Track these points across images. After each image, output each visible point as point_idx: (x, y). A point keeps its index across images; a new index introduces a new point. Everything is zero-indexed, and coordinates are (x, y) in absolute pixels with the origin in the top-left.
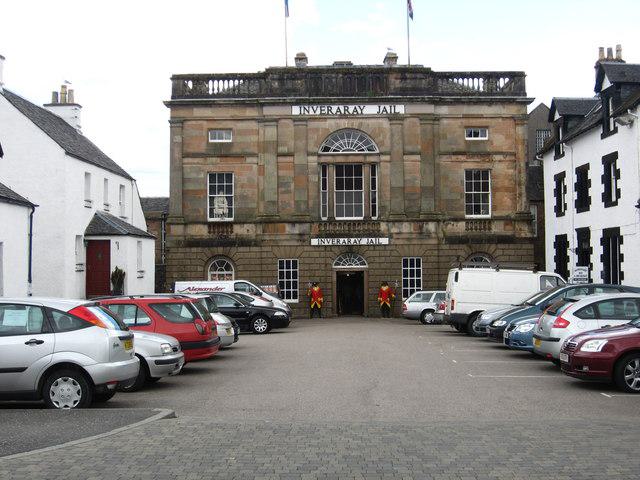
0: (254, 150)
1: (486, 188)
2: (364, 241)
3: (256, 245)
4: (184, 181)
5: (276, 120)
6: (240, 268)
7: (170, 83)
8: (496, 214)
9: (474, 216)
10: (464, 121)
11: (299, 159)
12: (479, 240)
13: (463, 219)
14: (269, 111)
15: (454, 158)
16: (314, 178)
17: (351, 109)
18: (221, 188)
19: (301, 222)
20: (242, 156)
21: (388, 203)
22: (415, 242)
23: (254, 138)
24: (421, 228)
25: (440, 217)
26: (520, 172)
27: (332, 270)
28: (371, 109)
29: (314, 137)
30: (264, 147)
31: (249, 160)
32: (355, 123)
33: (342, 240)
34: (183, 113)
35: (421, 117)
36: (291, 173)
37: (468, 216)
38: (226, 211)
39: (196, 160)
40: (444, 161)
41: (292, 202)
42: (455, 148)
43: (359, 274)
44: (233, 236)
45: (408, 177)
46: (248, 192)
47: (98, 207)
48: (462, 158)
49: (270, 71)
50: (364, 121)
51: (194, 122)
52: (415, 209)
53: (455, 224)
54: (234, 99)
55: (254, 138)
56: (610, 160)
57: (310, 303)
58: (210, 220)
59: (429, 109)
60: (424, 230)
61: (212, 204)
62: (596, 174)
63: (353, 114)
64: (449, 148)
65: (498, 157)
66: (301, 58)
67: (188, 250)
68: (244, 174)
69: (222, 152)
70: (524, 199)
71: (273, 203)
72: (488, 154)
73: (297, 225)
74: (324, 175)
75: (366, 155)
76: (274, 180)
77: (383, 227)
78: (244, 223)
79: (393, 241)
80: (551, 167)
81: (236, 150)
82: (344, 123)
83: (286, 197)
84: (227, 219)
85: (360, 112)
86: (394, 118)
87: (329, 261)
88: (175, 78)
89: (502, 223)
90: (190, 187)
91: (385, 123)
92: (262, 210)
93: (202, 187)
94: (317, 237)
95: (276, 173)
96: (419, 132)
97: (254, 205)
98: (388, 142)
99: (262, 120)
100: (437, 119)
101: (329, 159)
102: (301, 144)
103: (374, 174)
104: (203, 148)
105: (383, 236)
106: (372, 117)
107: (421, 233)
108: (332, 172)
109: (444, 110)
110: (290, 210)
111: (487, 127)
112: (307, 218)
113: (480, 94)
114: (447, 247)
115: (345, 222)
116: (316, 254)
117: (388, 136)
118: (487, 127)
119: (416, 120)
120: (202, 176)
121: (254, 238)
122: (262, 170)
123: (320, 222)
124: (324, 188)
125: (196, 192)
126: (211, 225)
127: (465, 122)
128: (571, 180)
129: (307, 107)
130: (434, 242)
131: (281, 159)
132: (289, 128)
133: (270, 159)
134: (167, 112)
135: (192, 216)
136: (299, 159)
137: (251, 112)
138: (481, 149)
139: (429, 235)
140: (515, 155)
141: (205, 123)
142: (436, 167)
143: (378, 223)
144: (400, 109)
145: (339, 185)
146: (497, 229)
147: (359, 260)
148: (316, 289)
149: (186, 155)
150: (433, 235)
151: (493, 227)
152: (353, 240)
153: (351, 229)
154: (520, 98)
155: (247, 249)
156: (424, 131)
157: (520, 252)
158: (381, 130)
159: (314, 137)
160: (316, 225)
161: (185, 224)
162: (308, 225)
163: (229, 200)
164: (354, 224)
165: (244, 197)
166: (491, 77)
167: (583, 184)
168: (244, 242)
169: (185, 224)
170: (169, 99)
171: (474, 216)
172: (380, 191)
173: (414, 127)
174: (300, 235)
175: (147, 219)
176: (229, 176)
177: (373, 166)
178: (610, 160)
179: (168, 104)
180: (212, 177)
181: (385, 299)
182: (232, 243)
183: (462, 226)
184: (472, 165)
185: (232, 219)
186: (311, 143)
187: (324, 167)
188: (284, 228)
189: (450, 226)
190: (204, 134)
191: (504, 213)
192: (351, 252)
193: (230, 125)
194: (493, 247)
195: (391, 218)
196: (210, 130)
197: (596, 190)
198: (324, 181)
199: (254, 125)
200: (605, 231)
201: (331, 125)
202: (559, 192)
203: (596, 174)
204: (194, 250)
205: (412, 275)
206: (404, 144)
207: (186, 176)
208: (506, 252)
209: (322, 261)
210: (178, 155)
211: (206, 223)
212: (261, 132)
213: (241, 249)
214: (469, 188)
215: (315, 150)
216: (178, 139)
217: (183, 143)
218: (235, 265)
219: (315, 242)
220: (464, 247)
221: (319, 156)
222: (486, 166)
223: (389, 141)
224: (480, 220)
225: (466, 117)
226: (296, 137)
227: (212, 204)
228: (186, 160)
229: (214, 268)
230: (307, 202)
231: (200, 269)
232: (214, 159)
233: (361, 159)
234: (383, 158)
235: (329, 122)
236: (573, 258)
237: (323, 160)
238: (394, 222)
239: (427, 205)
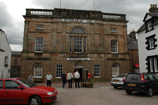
0: (50, 31)
2: (83, 59)
4: (28, 40)
6: (44, 67)
7: (25, 11)
8: (120, 52)
9: (113, 53)
10: (110, 26)
11: (64, 34)
13: (111, 53)
14: (55, 20)
15: (108, 36)
17: (79, 20)
19: (63, 53)
20: (46, 33)
21: (90, 48)
24: (100, 55)
25: (105, 53)
26: (125, 41)
28: (85, 21)
30: (53, 30)
31: (48, 34)
32: (80, 25)
33: (76, 59)
35: (99, 24)
36: (61, 38)
37: (112, 53)
39: (32, 34)
40: (106, 37)
41: (61, 47)
44: (42, 57)
48: (110, 36)
49: (55, 9)
50: (83, 24)
51: (32, 23)
52: (98, 50)
53: (109, 54)
55: (50, 28)
58: (35, 52)
59: (101, 22)
60: (100, 56)
63: (80, 22)
64: (106, 33)
67: (28, 61)
69: (41, 32)
70: (127, 48)
71: (56, 47)
72: (117, 35)
75: (83, 34)
77: (88, 55)
78: (46, 53)
81: (44, 31)
82: (77, 25)
84: (40, 52)
85: (82, 21)
86: (91, 24)
87: (72, 65)
88: (27, 10)
89: (121, 55)
90: (29, 41)
91: (89, 25)
92: (51, 49)
93: (34, 42)
94: (69, 57)
95: (56, 38)
96: (98, 28)
100: (103, 25)
101: (72, 35)
103: (85, 40)
104: (34, 31)
107: (100, 57)
109: (105, 23)
110: (60, 50)
111: (116, 28)
114: (107, 61)
116: (68, 63)
117: (90, 29)
118: (116, 28)
120: (34, 38)
121: (49, 58)
122: (52, 37)
126: (36, 53)
127: (111, 26)
129: (66, 19)
130: (104, 60)
131: (58, 34)
132: (60, 25)
133: (55, 34)
134: (24, 20)
135: (30, 50)
136: (64, 34)
138: (115, 34)
139: (102, 58)
140: (124, 36)
141: (35, 23)
143: (87, 54)
144: (93, 21)
146: (120, 56)
147: (81, 65)
149: (28, 32)
151: (119, 56)
152: (80, 59)
155: (47, 61)
156: (100, 28)
157: (126, 63)
160: (68, 54)
161: (28, 53)
162: (66, 54)
164: (80, 54)
165: (46, 45)
168: (46, 59)
169: (28, 53)
170: (25, 15)
171: (113, 53)
172: (87, 44)
174: (63, 57)
176: (42, 39)
179: (24, 16)
181: (89, 77)
182: (41, 59)
183: (111, 55)
184: (113, 38)
185: (42, 52)
189: (107, 56)
190: (35, 25)
191: (122, 52)
193: (43, 24)
195: (91, 52)
196: (37, 25)
199: (50, 24)
201: (73, 25)
204: (30, 61)
205: (97, 70)
206: (94, 31)
207: (29, 38)
208: (123, 63)
210: (26, 32)
211: (34, 53)
212: (52, 26)
213: (45, 61)
215: (68, 32)
216: (27, 27)
217: (28, 29)
218: (42, 66)
219: (68, 59)
222: (117, 39)
223: (90, 30)
225: (111, 25)
228: (29, 33)
229: (36, 67)
230: (65, 47)
234: (89, 35)
235: (72, 24)
237: (71, 35)
238: (92, 53)
239: (101, 49)
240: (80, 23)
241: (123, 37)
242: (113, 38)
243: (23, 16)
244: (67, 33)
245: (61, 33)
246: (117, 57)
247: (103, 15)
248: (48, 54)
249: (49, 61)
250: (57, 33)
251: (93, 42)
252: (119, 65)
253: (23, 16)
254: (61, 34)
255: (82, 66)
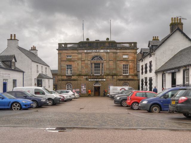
0: (77, 60)
1: (127, 68)
2: (100, 80)
3: (77, 81)
5: (81, 53)
10: (123, 53)
11: (86, 62)
12: (125, 80)
13: (122, 75)
14: (80, 51)
15: (120, 62)
16: (89, 66)
17: (98, 51)
18: (69, 68)
20: (73, 61)
22: (111, 80)
23: (76, 57)
24: (113, 77)
27: (93, 86)
28: (102, 51)
29: (89, 57)
30: (79, 59)
31: (75, 62)
34: (61, 52)
35: (113, 53)
38: (70, 73)
39: (64, 62)
40: (118, 62)
42: (120, 59)
43: (99, 88)
45: (110, 66)
46: (75, 69)
47: (40, 72)
48: (122, 62)
49: (79, 43)
50: (101, 54)
54: (72, 49)
55: (76, 57)
56: (151, 63)
57: (88, 93)
59: (115, 51)
61: (67, 71)
62: (148, 65)
65: (130, 62)
66: (88, 39)
67: (62, 81)
68: (74, 65)
69: (70, 60)
71: (81, 71)
72: (128, 61)
73: (86, 76)
74: (92, 65)
75: (101, 61)
76: (81, 66)
77: (105, 77)
79: (106, 80)
80: (141, 64)
81: (73, 60)
82: (96, 54)
83: (83, 70)
86: (107, 53)
88: (59, 44)
90: (63, 68)
91: (105, 54)
97: (76, 72)
98: (106, 58)
99: (79, 53)
100: (116, 53)
101: (93, 62)
102: (87, 59)
103: (103, 65)
104: (65, 59)
105: (104, 79)
106: (101, 53)
108: (93, 65)
109: (118, 51)
112: (88, 75)
113: (127, 47)
115: (96, 76)
116: (90, 83)
117: (106, 56)
119: (112, 53)
123: (91, 76)
124: (92, 68)
125: (64, 69)
126: (67, 76)
128: (144, 67)
131: (82, 62)
132: (84, 55)
133: (80, 62)
134: (57, 51)
136: (86, 62)
137: (76, 51)
140: (134, 61)
141: (66, 54)
142: (116, 64)
144: (108, 51)
145: (95, 67)
146: (130, 77)
148: (89, 90)
150: (115, 79)
151: (129, 77)
153: (97, 77)
154: (135, 48)
155: (75, 81)
158: (104, 55)
159: (89, 57)
163: (71, 70)
166: (130, 43)
167: (146, 68)
168: (74, 80)
173: (112, 55)
175: (53, 75)
176: (71, 66)
177: (102, 63)
178: (151, 63)
180: (67, 66)
182: (71, 80)
183: (122, 76)
184: (124, 63)
185: (71, 75)
186: (89, 58)
187: (92, 63)
188: (83, 77)
190: (65, 56)
192: (97, 82)
193: (71, 54)
194: (129, 81)
196: (67, 55)
197: (148, 69)
198: (92, 67)
199: (76, 54)
200: (150, 78)
201: (93, 54)
202: (142, 69)
203: (148, 65)
204: (63, 81)
209: (91, 84)
210: (60, 61)
211: (66, 76)
213: (73, 81)
214: (124, 68)
216: (60, 57)
219: (89, 80)
220: (123, 81)
221: (91, 61)
224: (126, 75)
226: (85, 57)
227: (67, 71)
228: (61, 62)
230: (88, 71)
231: (64, 86)
232: (68, 62)
233: (99, 62)
236: (144, 84)
237: (91, 62)
239: (114, 72)
240: (98, 52)
241: (133, 62)
242: (124, 63)
243: (57, 49)
244: (88, 61)
245: (85, 61)
246: (127, 78)
247: (117, 44)
248: (76, 77)
249: (76, 81)
250: (82, 61)
251: (108, 67)
252: (129, 84)
253: (57, 49)
254: (84, 62)
255: (100, 85)
